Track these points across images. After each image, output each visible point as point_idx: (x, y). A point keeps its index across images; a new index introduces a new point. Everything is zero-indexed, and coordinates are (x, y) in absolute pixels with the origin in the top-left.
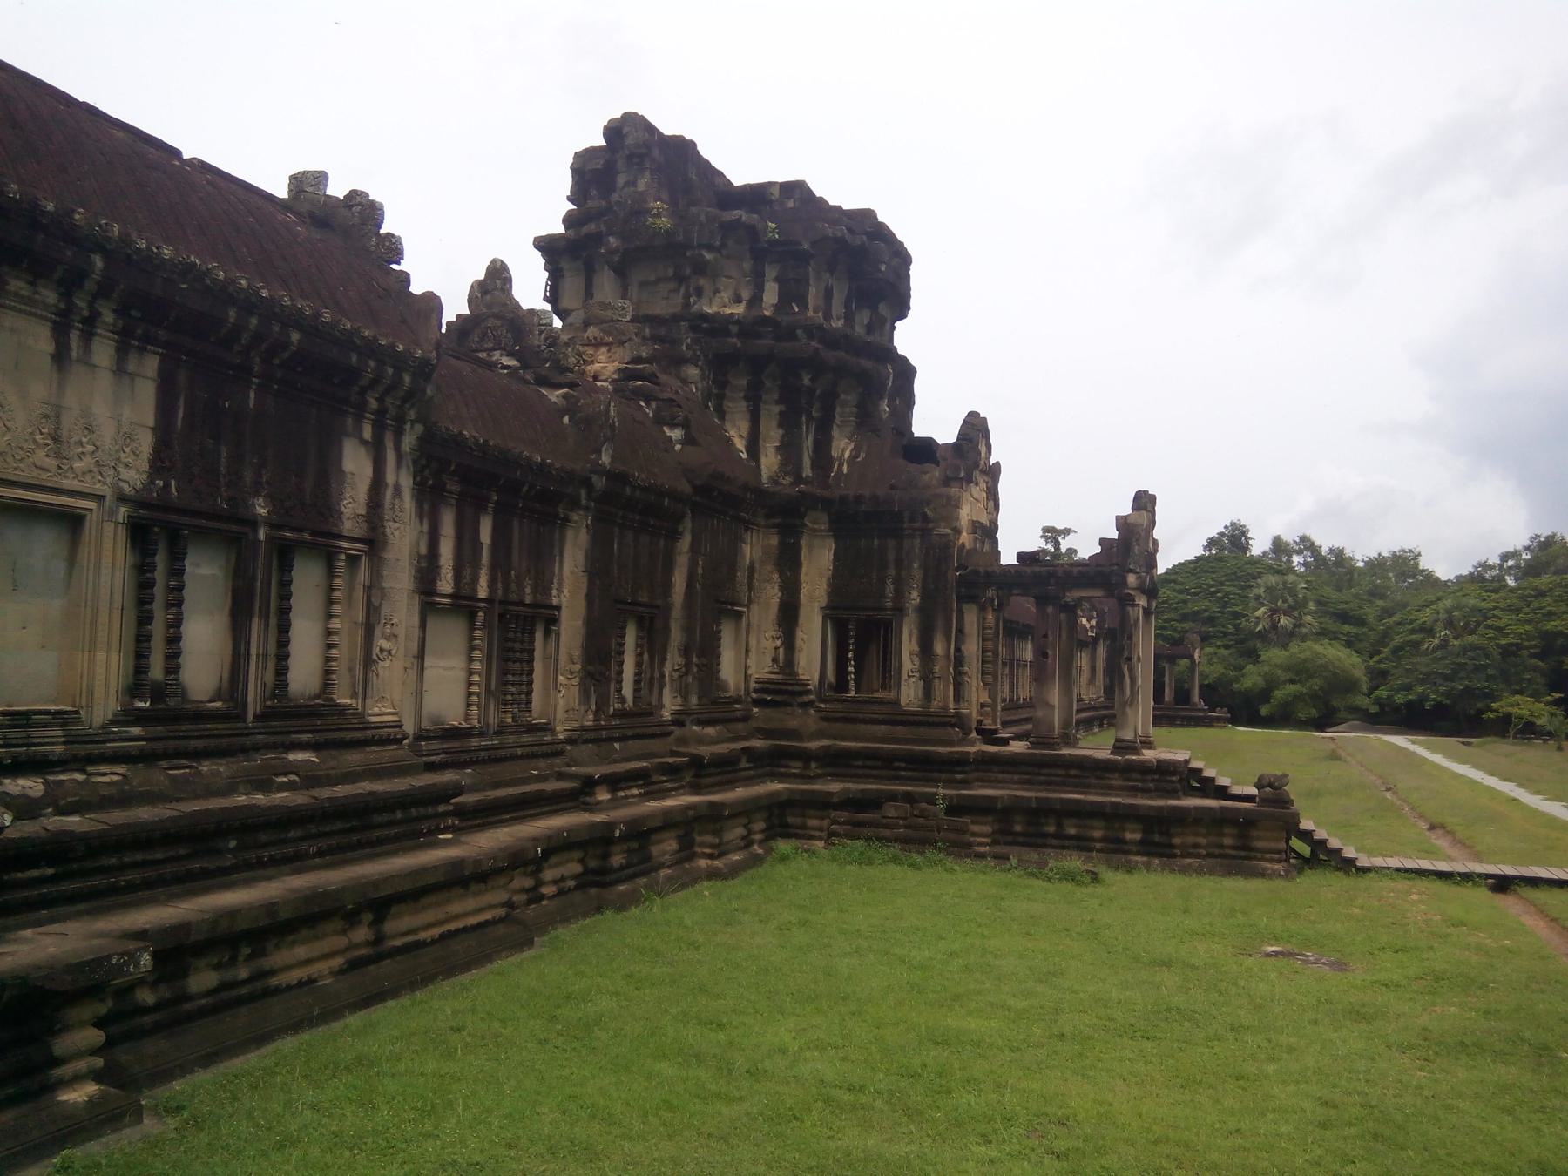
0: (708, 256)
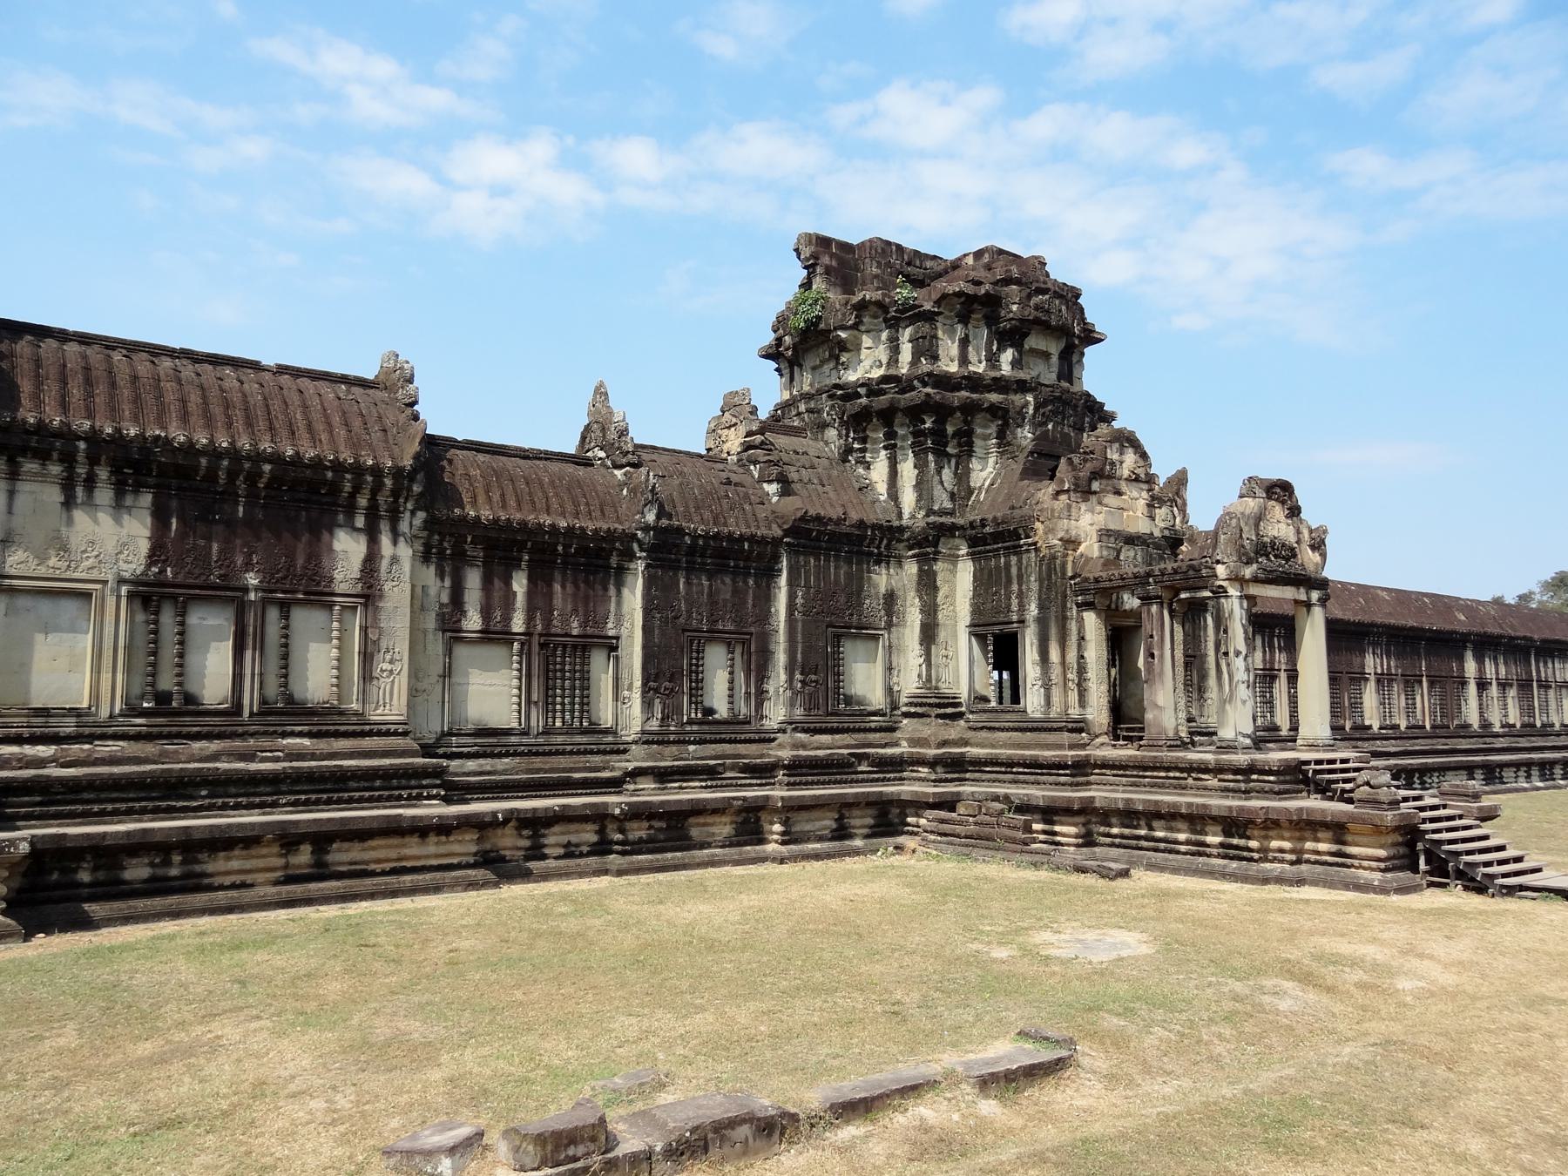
0: (843, 335)
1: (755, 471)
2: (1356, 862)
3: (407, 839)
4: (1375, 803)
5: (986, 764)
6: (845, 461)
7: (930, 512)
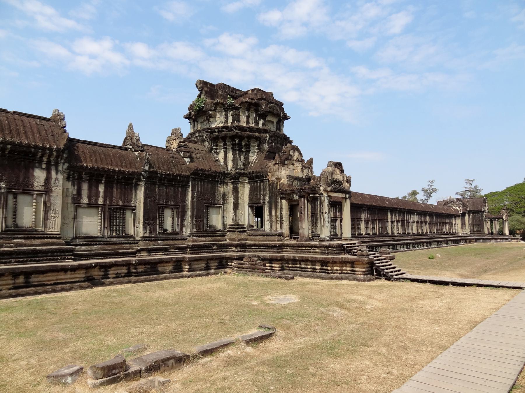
0: (211, 113)
1: (182, 154)
2: (357, 273)
3: (60, 273)
4: (362, 255)
5: (252, 246)
6: (211, 152)
7: (237, 169)
